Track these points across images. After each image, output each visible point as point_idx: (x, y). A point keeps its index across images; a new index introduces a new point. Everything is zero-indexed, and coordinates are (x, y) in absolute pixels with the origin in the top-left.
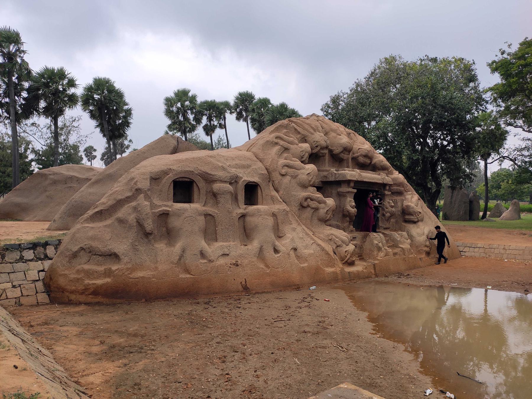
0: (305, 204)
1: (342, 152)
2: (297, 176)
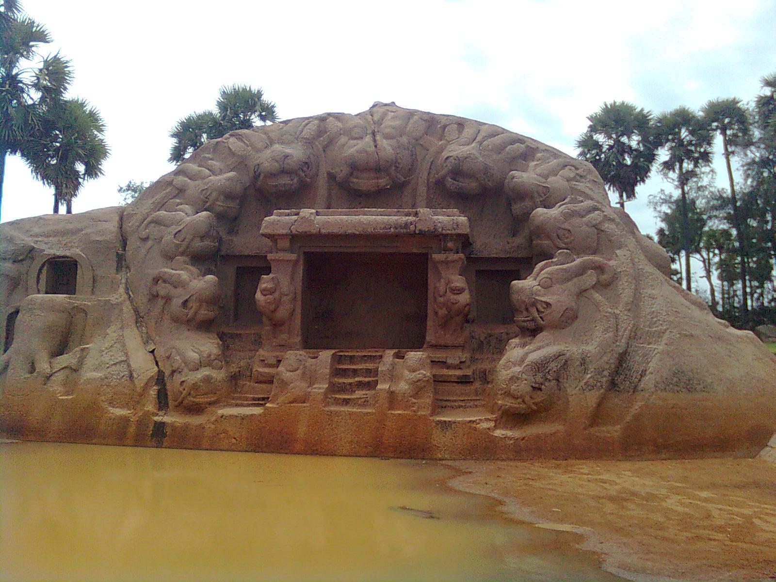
0: (155, 289)
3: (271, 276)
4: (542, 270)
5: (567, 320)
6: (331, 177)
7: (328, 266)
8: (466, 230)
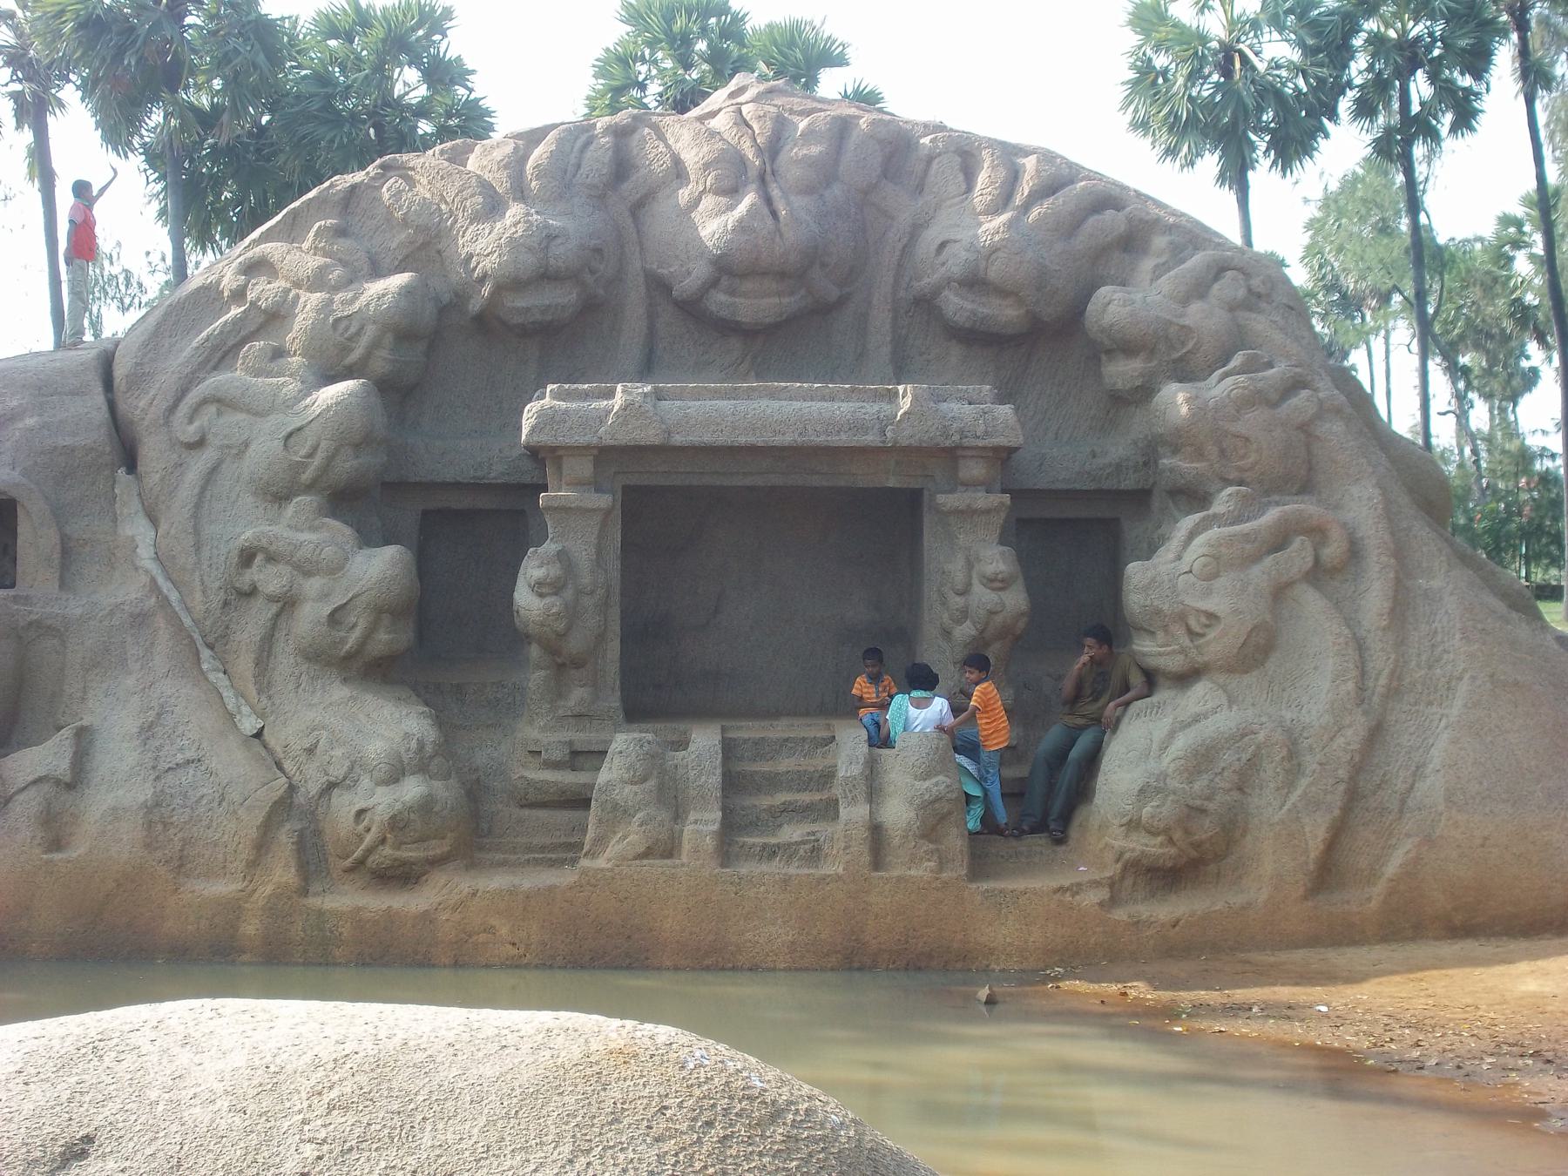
1: (713, 284)
2: (246, 444)
4: (1192, 535)
6: (659, 286)
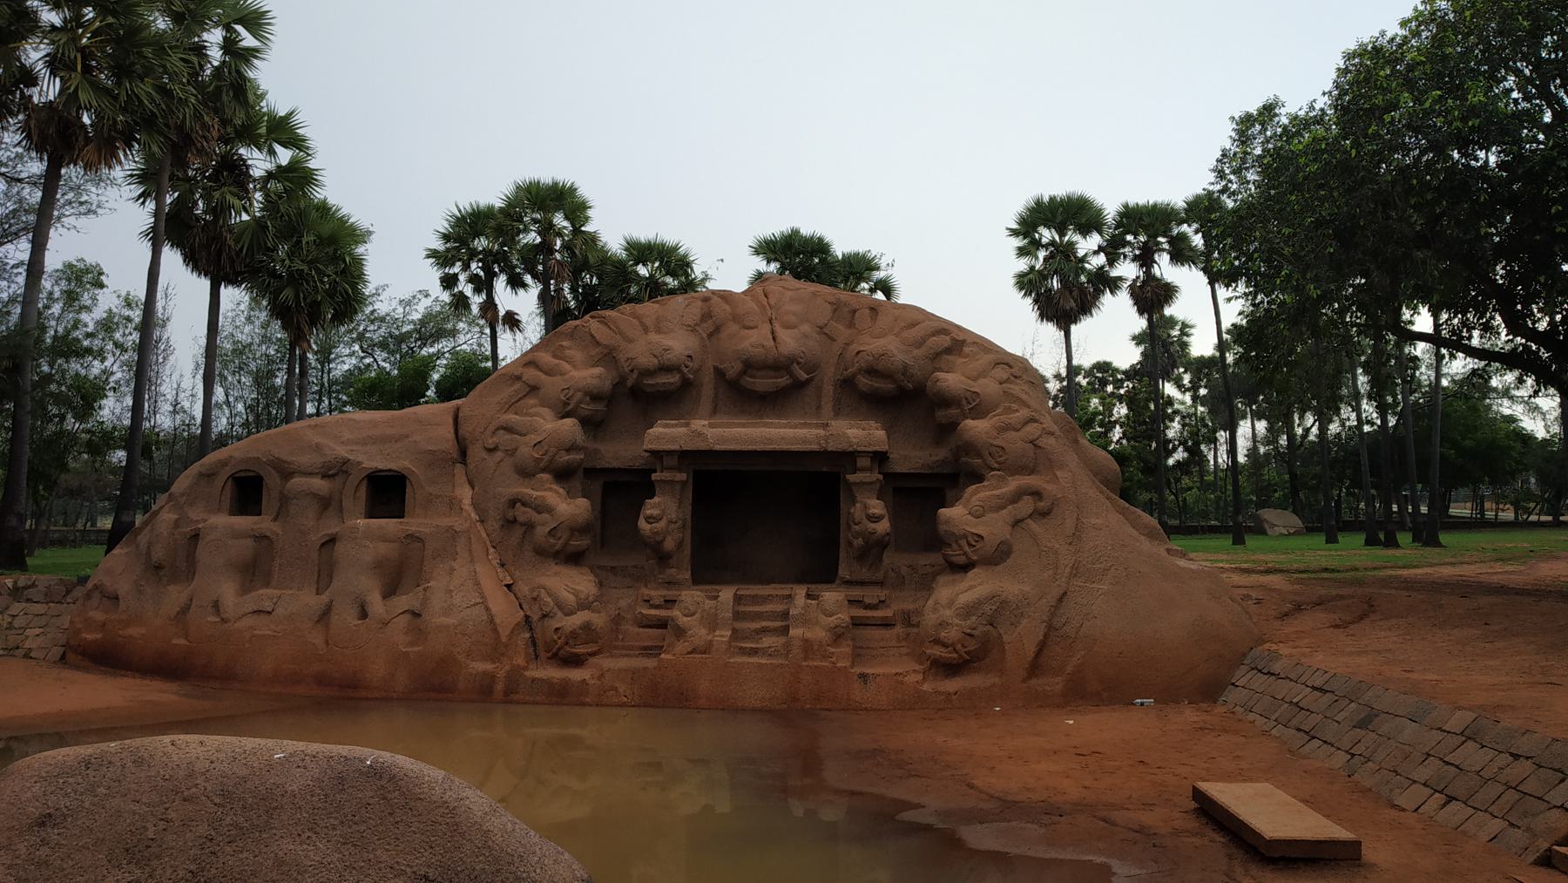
0: (510, 514)
3: (656, 499)
5: (999, 556)
7: (720, 484)
8: (885, 448)
